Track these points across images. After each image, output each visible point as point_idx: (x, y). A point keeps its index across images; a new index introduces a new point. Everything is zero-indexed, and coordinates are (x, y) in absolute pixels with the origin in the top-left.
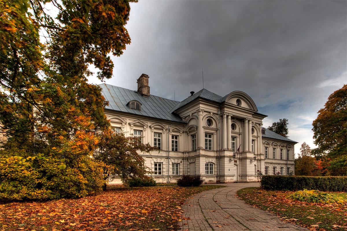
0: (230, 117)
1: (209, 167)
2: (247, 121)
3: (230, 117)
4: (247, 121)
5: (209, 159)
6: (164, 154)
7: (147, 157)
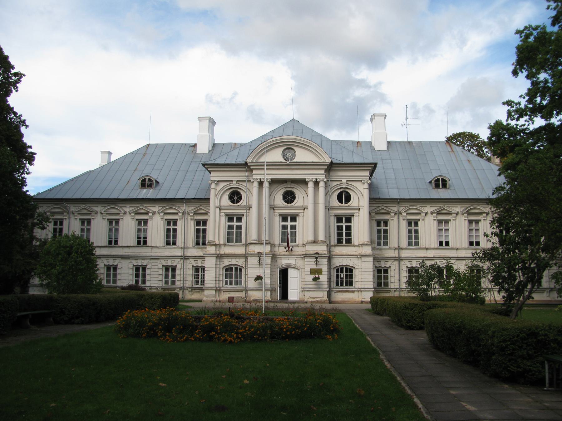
0: (266, 184)
1: (234, 273)
2: (311, 184)
3: (266, 184)
4: (311, 184)
5: (230, 260)
6: (178, 252)
7: (151, 258)
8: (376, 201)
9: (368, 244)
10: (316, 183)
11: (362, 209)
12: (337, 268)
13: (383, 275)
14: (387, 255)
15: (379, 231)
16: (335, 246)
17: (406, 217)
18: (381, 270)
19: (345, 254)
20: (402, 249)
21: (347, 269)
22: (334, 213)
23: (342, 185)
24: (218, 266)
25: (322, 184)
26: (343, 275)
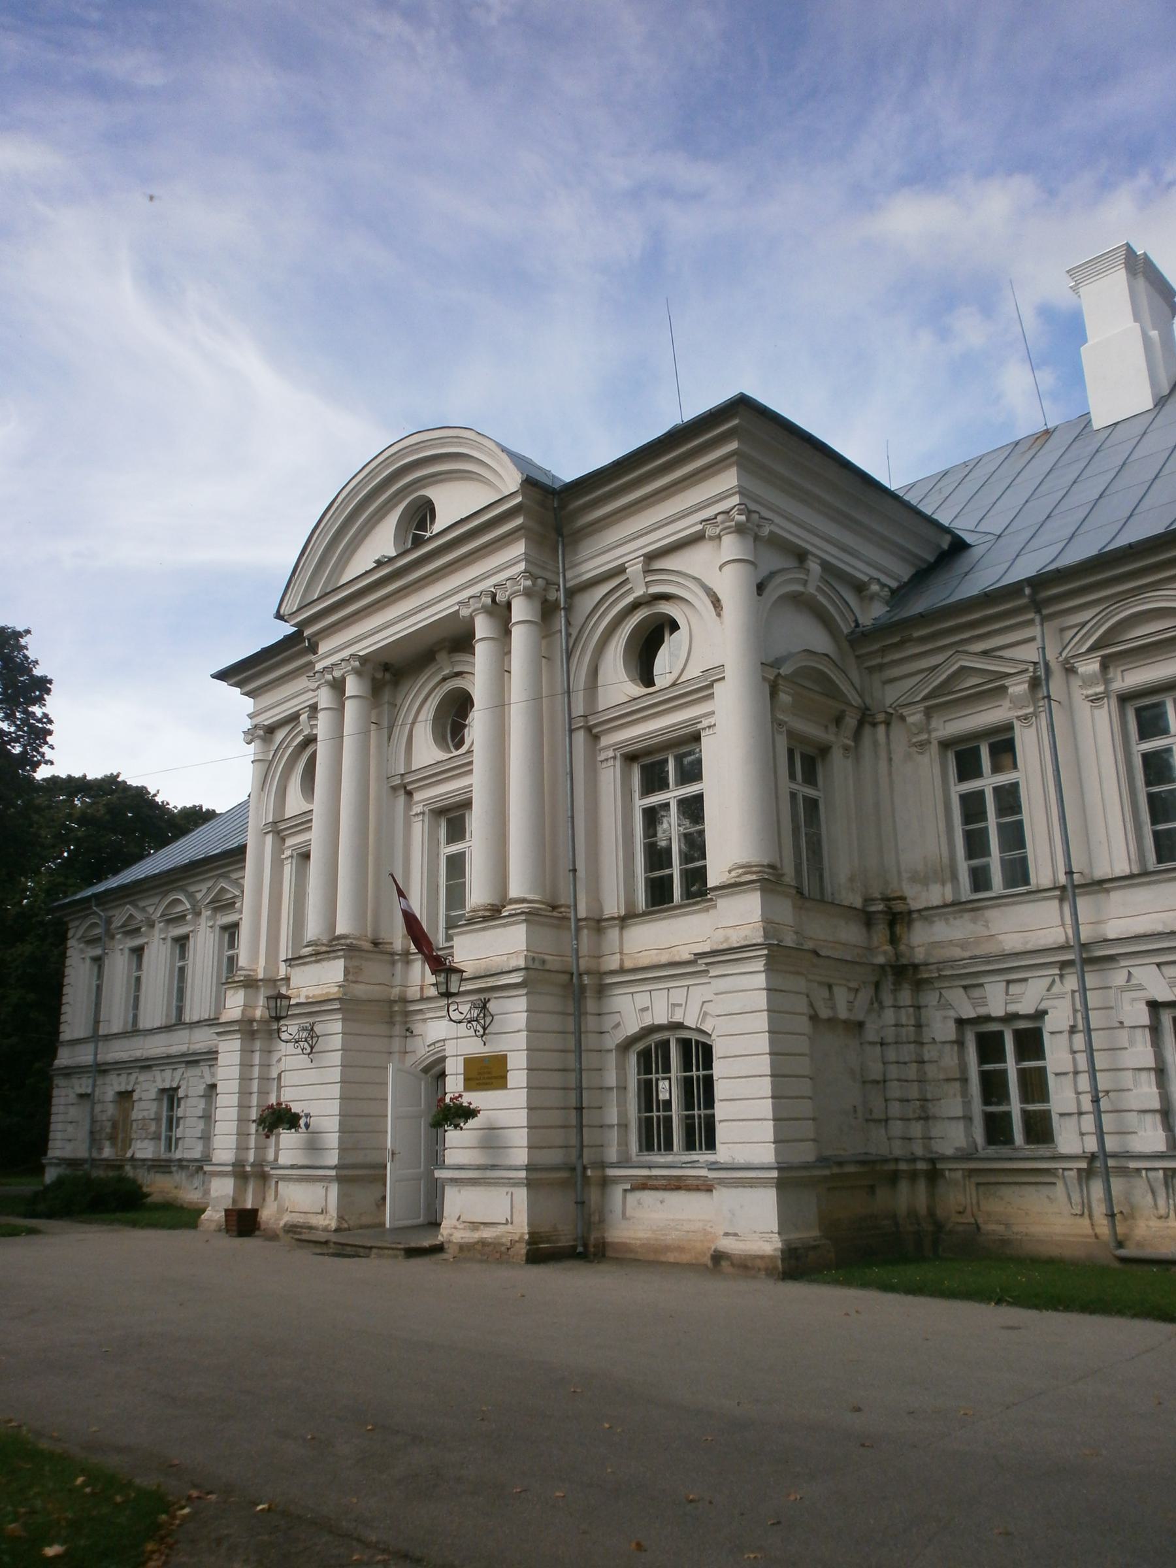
3: (352, 686)
4: (482, 627)
8: (916, 634)
9: (742, 879)
10: (500, 612)
11: (721, 684)
12: (640, 1046)
13: (1011, 1066)
14: (1012, 943)
15: (973, 807)
16: (627, 919)
17: (1107, 682)
18: (1000, 1035)
19: (664, 958)
20: (1100, 885)
21: (685, 1044)
22: (616, 747)
23: (631, 590)
24: (256, 1072)
25: (520, 610)
26: (667, 1082)
